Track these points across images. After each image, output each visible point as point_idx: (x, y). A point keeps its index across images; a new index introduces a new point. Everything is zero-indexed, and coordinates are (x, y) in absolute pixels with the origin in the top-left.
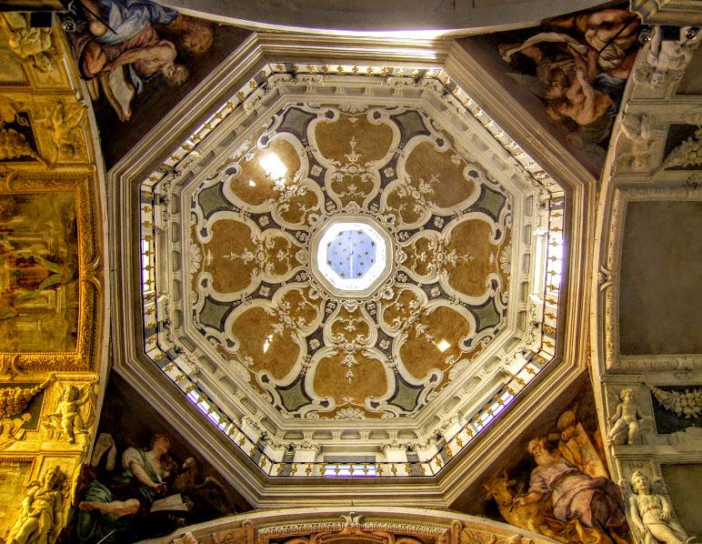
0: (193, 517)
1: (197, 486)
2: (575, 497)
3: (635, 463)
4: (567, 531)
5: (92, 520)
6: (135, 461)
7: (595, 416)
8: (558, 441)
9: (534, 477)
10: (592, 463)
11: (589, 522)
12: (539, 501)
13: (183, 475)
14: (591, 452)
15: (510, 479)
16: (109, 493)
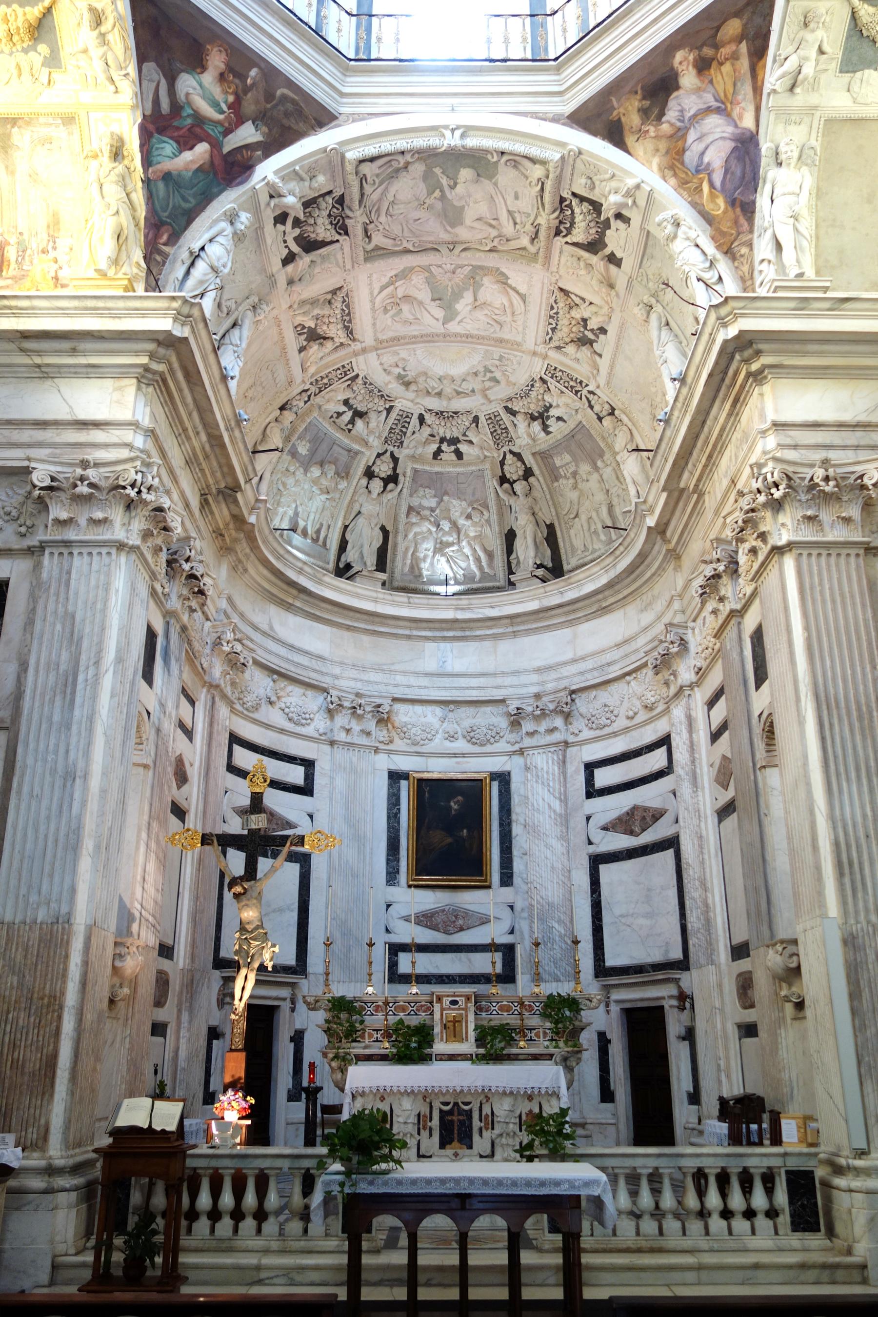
0: (271, 147)
1: (269, 106)
2: (712, 142)
3: (793, 118)
4: (692, 186)
5: (167, 185)
6: (191, 91)
7: (768, 34)
8: (713, 59)
9: (672, 103)
10: (743, 105)
11: (718, 183)
12: (671, 136)
13: (249, 95)
14: (747, 88)
15: (644, 98)
16: (175, 145)
